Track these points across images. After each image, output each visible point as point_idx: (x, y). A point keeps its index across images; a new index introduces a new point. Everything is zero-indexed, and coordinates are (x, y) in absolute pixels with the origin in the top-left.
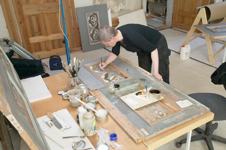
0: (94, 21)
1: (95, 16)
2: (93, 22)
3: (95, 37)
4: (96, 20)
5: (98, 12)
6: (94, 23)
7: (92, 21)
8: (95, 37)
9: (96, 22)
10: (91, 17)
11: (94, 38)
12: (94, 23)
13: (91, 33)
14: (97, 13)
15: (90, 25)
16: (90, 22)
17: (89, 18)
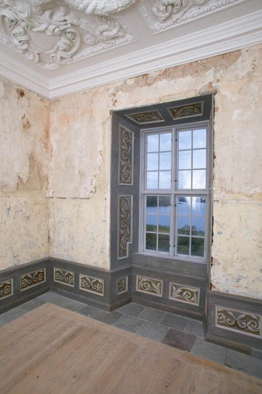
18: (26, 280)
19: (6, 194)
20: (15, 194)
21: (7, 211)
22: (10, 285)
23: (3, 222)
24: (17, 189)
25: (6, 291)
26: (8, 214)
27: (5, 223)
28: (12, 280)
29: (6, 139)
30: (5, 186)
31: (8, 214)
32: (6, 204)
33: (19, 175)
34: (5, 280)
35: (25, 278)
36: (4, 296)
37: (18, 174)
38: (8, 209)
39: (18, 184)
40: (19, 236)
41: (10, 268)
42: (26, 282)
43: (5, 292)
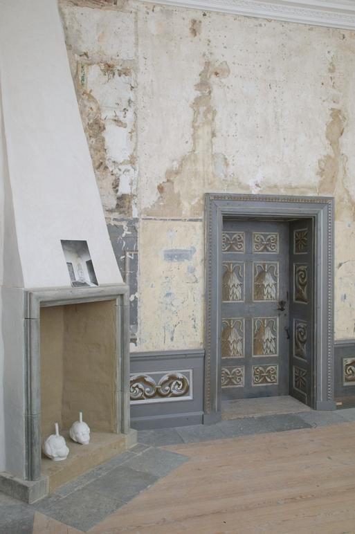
0: (172, 387)
1: (183, 392)
2: (170, 386)
3: (137, 386)
4: (175, 392)
5: (190, 398)
6: (167, 388)
7: (174, 383)
8: (137, 386)
9: (170, 392)
10: (182, 380)
11: (134, 385)
12: (167, 388)
13: (147, 379)
14: (189, 395)
15: (166, 378)
16: (172, 378)
17: (180, 376)
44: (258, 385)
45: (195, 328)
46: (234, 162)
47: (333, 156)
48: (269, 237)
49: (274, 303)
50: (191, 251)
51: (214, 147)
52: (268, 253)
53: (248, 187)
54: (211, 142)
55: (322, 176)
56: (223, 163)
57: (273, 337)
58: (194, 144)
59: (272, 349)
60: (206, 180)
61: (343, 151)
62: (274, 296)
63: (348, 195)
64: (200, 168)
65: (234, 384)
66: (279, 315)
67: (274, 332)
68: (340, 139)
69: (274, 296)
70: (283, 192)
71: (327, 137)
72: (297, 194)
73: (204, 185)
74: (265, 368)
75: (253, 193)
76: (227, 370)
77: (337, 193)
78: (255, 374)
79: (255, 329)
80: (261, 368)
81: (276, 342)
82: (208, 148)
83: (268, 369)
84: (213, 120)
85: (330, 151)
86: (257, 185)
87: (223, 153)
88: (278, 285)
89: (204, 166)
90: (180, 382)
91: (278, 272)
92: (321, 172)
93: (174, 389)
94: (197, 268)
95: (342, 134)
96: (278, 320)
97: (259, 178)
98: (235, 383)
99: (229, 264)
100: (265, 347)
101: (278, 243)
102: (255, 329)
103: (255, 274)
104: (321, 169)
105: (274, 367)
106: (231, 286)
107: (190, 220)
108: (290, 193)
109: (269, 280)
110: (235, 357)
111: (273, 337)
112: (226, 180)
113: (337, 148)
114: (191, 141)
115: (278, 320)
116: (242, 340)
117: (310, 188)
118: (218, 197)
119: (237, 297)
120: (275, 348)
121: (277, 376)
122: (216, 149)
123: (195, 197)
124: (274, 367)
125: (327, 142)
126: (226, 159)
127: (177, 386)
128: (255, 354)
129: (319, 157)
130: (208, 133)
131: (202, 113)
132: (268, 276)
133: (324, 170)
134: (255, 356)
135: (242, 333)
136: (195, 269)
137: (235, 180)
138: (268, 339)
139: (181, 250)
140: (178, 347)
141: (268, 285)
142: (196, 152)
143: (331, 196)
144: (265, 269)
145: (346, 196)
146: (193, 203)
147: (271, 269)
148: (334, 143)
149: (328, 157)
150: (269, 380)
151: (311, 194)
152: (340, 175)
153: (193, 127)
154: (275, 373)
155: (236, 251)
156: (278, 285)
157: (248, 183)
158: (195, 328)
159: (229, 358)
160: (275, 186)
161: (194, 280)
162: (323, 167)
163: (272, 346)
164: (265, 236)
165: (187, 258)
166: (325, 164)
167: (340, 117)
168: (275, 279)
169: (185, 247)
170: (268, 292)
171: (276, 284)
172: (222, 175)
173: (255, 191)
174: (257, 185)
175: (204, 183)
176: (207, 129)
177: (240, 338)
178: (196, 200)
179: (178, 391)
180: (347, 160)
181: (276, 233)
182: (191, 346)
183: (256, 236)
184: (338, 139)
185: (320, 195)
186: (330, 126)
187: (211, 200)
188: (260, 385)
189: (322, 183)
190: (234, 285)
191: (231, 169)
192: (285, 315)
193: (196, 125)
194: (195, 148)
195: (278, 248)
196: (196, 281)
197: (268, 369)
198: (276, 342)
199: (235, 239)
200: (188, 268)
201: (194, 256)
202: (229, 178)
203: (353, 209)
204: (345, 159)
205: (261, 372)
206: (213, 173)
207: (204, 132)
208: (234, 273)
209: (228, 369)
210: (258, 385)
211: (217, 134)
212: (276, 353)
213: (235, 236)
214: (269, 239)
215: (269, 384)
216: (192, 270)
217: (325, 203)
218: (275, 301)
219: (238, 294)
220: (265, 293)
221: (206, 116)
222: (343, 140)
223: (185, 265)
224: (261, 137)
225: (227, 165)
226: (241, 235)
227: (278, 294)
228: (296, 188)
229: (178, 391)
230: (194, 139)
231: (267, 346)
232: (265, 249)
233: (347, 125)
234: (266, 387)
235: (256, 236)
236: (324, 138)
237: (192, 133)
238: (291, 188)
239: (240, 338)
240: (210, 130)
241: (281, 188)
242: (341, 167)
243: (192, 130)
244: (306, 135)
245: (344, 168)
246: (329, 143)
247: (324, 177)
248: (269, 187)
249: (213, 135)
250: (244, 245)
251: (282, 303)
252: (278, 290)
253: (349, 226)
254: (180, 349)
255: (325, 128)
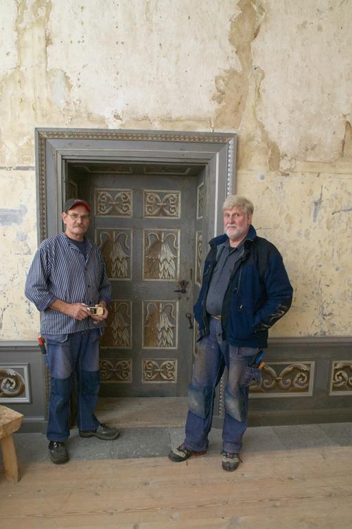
17: (12, 372)
18: (345, 375)
19: (313, 167)
20: (334, 166)
21: (313, 207)
22: (308, 373)
23: (303, 232)
24: (342, 155)
25: (297, 382)
26: (315, 216)
27: (307, 235)
28: (313, 364)
29: (320, 28)
30: (313, 149)
31: (315, 216)
32: (311, 192)
33: (348, 119)
34: (297, 360)
35: (343, 369)
36: (292, 391)
37: (345, 116)
38: (316, 204)
39: (344, 143)
40: (337, 269)
41: (310, 337)
42: (344, 379)
43: (296, 386)
44: (150, 382)
45: (30, 313)
46: (79, 83)
47: (239, 70)
48: (167, 196)
49: (173, 283)
50: (20, 211)
51: (49, 59)
52: (166, 218)
53: (103, 120)
54: (46, 52)
55: (220, 103)
56: (64, 84)
57: (171, 325)
58: (19, 56)
59: (169, 340)
60: (38, 111)
61: (257, 62)
62: (172, 273)
63: (263, 131)
64: (29, 92)
65: (119, 379)
66: (180, 298)
67: (172, 320)
68: (252, 44)
69: (172, 273)
70: (157, 126)
71: (230, 40)
72: (179, 128)
73: (36, 118)
74: (160, 362)
75: (111, 127)
76: (109, 362)
77: (245, 128)
78: (146, 369)
79: (145, 316)
80: (154, 363)
81: (174, 332)
82: (41, 63)
83: (163, 364)
84: (47, 16)
85: (235, 63)
86: (117, 117)
87: (64, 69)
88: (179, 260)
89: (35, 89)
90: (12, 380)
91: (179, 244)
92: (220, 97)
93: (5, 387)
94: (29, 235)
95: (255, 37)
96: (178, 303)
97: (119, 106)
98: (121, 378)
99: (111, 232)
100: (160, 337)
101: (180, 204)
102: (145, 316)
103: (147, 245)
104: (219, 91)
105: (171, 362)
106: (114, 260)
107: (18, 168)
108: (167, 128)
109: (166, 253)
110: (121, 348)
111: (171, 325)
112: (69, 110)
113: (248, 58)
114: (14, 51)
115: (178, 303)
116: (129, 327)
117: (200, 120)
118: (58, 134)
119: (121, 274)
120: (174, 339)
121: (175, 374)
122: (52, 63)
123: (24, 135)
124: (171, 362)
125: (230, 48)
126: (67, 78)
127: (8, 385)
128: (145, 345)
129: (217, 73)
130: (39, 38)
131: (29, 7)
132: (165, 249)
133: (223, 93)
134: (145, 348)
135: (130, 319)
136: (26, 236)
137: (82, 110)
138: (164, 328)
139: (6, 210)
140: (9, 336)
141: (166, 260)
142: (21, 69)
143: (232, 131)
144: (160, 239)
145: (259, 132)
146: (21, 144)
147: (170, 240)
148: (243, 50)
149: (232, 73)
150: (165, 377)
151: (202, 129)
152: (250, 101)
153: (17, 30)
154: (173, 370)
155: (120, 214)
156: (179, 260)
157: (102, 114)
158: (30, 313)
159: (111, 348)
160: (146, 118)
161: (26, 251)
162: (222, 88)
163: (169, 336)
164: (162, 195)
165: (16, 221)
166: (226, 85)
167: (255, 7)
168: (175, 251)
169: (11, 205)
170: (164, 268)
171: (175, 259)
172: (62, 103)
173: (114, 125)
174: (117, 117)
175: (36, 114)
176: (39, 32)
177: (126, 325)
178: (25, 139)
179: (10, 390)
180: (263, 78)
181: (177, 191)
182: (26, 336)
183: (149, 194)
184: (249, 45)
185: (216, 131)
186: (236, 23)
187: (43, 140)
188: (155, 382)
189: (220, 114)
190: (118, 259)
191: (76, 93)
192: (188, 299)
193: (22, 26)
194: (21, 62)
195: (179, 212)
196: (29, 252)
197: (163, 364)
198: (174, 332)
199: (119, 199)
200: (17, 235)
201: (24, 218)
202: (72, 107)
203: (270, 152)
204: (260, 74)
205: (155, 367)
206: (49, 100)
207: (34, 37)
208: (119, 244)
209: (110, 361)
210: (150, 382)
211: (56, 41)
212: (174, 346)
213: (119, 194)
214: (167, 199)
215: (165, 382)
216: (24, 238)
217: (219, 141)
218: (173, 280)
219: (123, 271)
220: (161, 269)
221: (36, 13)
222: (257, 44)
223: (12, 230)
224: (123, 43)
225: (70, 87)
226: (126, 193)
227: (178, 271)
228: (178, 120)
229: (10, 390)
230: (19, 49)
231: (162, 336)
232: (162, 212)
233: (266, 20)
234: (161, 385)
235: (149, 194)
236: (226, 43)
237: (16, 39)
238: (170, 120)
239: (126, 325)
240: (42, 35)
241: (154, 120)
242: (251, 88)
243: (15, 34)
244: (197, 38)
245: (258, 90)
246: (235, 50)
247: (224, 103)
248: (137, 120)
249: (48, 41)
250: (131, 207)
251: (183, 283)
252: (178, 267)
253: (262, 178)
254: (12, 339)
255: (228, 27)
